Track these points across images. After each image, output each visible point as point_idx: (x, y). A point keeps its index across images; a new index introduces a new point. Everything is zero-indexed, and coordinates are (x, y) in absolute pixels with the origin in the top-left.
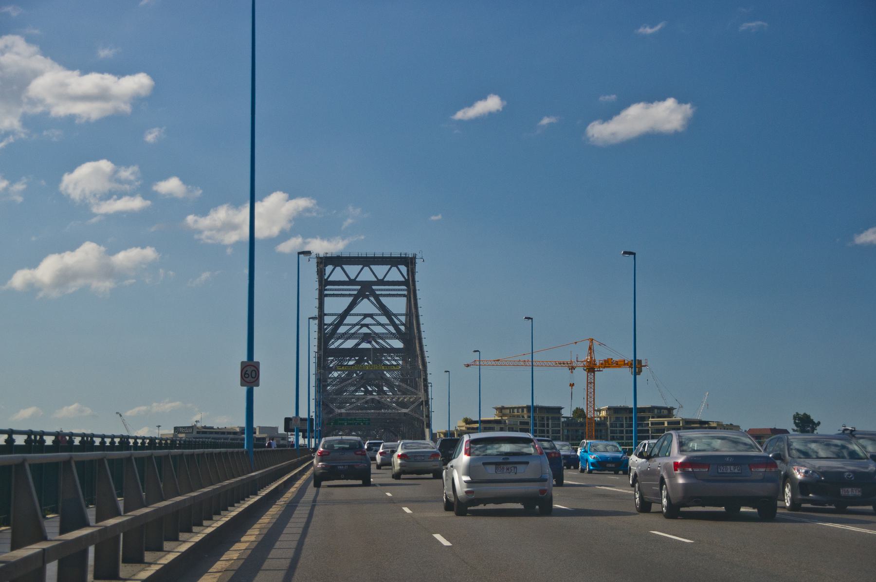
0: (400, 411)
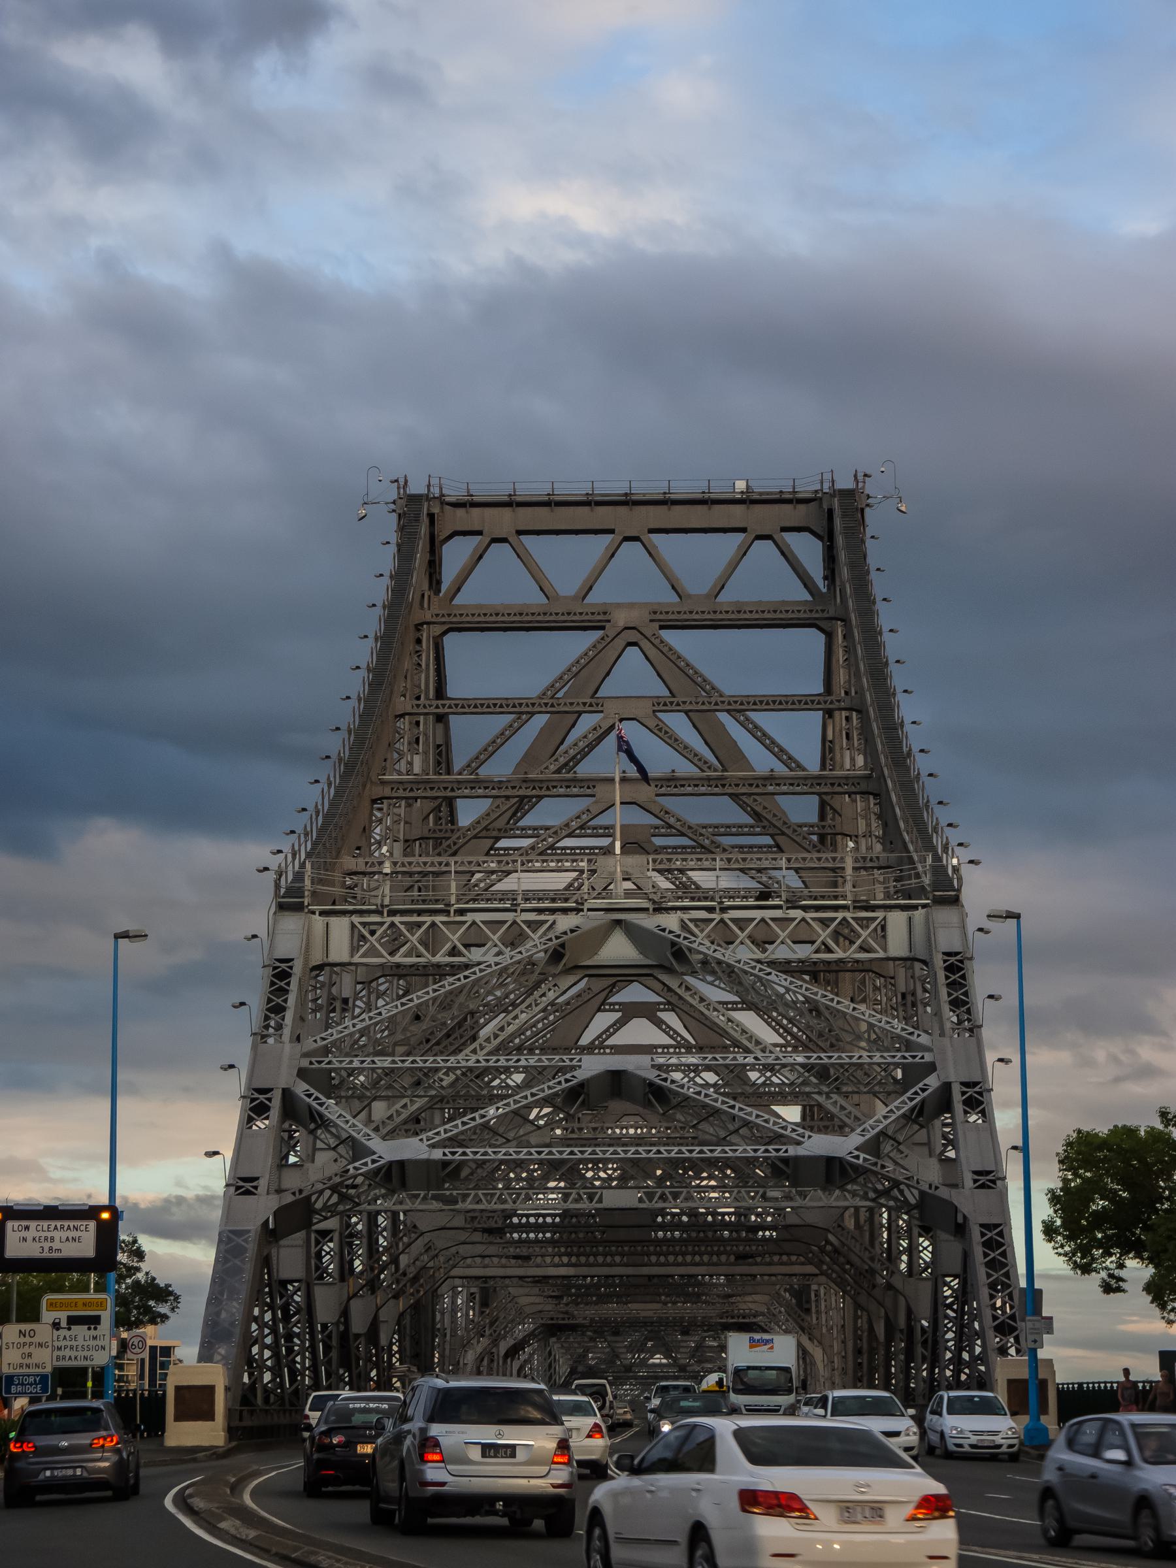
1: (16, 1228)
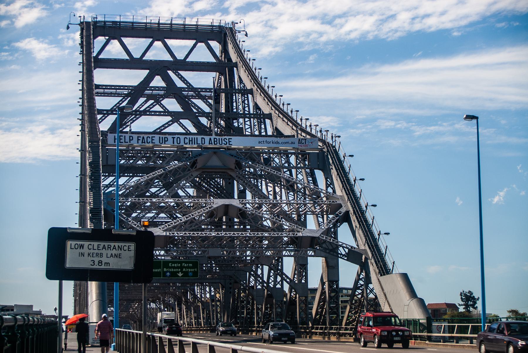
0: (300, 234)
1: (73, 247)
